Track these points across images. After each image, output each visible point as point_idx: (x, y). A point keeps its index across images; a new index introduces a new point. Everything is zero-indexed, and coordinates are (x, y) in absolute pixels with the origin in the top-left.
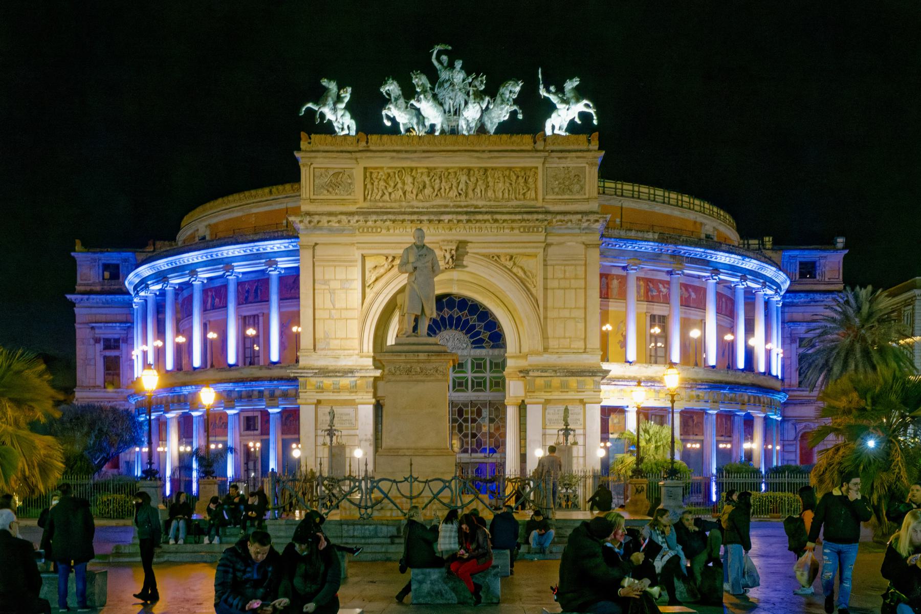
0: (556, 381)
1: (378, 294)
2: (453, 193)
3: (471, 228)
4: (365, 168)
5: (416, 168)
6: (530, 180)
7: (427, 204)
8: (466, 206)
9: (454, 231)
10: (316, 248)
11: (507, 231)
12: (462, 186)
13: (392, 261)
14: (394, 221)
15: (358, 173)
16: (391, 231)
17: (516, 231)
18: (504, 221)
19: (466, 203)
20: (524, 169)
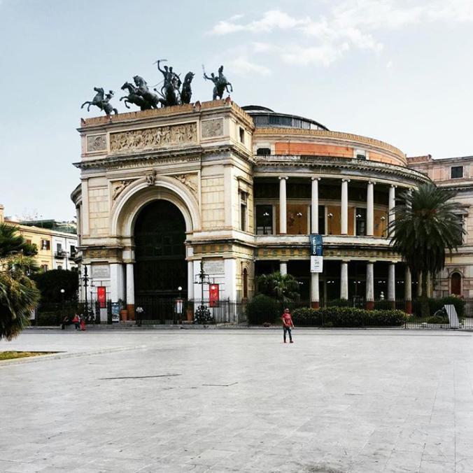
0: (208, 248)
1: (118, 203)
2: (154, 143)
3: (162, 162)
4: (111, 134)
5: (136, 130)
6: (194, 130)
7: (141, 150)
8: (160, 149)
9: (154, 164)
10: (89, 180)
11: (181, 161)
12: (159, 137)
13: (125, 184)
14: (123, 162)
15: (108, 137)
16: (123, 167)
17: (185, 161)
18: (178, 156)
19: (159, 148)
20: (189, 123)
